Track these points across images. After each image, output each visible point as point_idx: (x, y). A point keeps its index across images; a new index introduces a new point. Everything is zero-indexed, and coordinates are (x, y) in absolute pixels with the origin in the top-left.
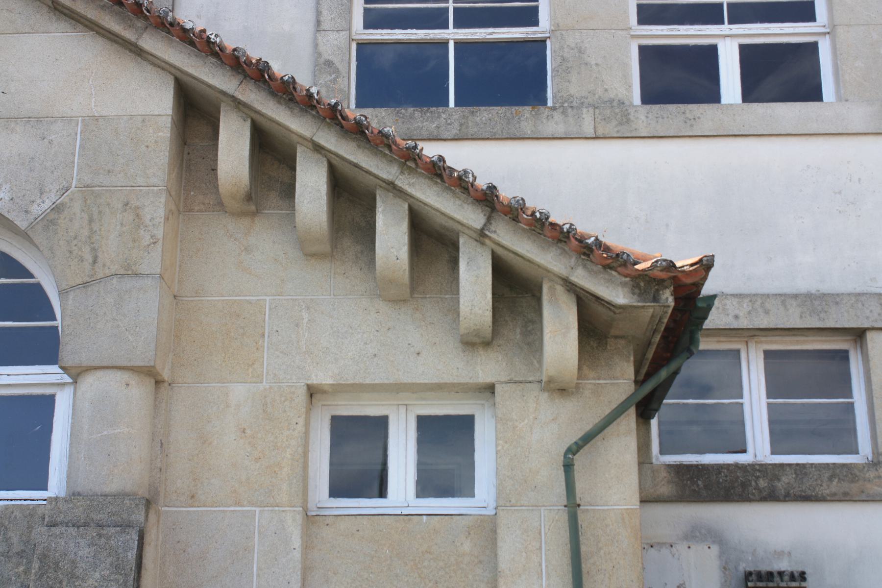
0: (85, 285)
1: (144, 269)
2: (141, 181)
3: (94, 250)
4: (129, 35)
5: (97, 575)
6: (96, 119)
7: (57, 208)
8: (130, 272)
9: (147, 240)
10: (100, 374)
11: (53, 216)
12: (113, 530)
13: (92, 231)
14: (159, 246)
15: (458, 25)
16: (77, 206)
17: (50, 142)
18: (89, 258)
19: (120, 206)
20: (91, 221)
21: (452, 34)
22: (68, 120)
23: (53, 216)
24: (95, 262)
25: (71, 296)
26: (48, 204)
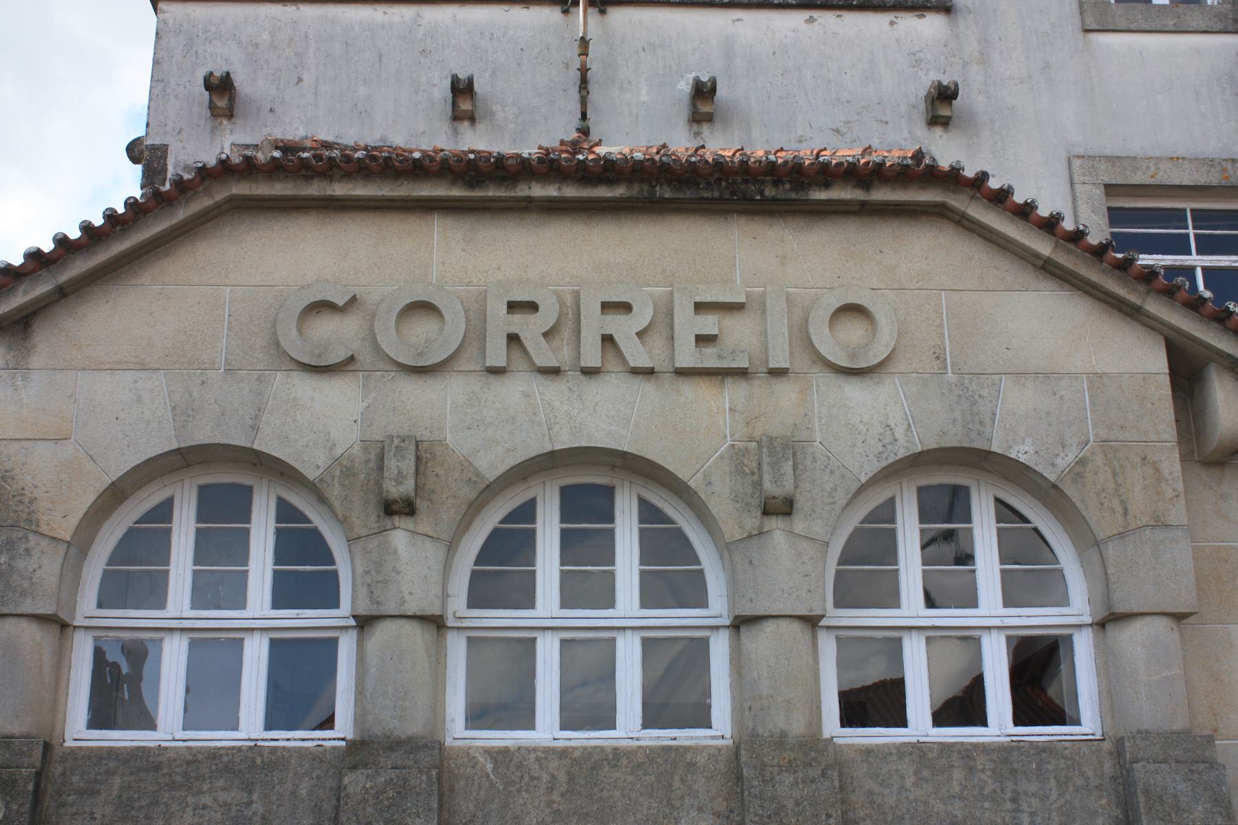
0: (1121, 535)
1: (1172, 520)
2: (1153, 437)
3: (1123, 502)
4: (1133, 298)
5: (1200, 808)
6: (1100, 376)
7: (1082, 462)
8: (1159, 524)
9: (1169, 494)
10: (1148, 619)
11: (1078, 469)
12: (1202, 766)
13: (1118, 485)
14: (1182, 500)
15: (1200, 252)
16: (1099, 460)
17: (1062, 397)
18: (1119, 509)
19: (1139, 460)
20: (1114, 474)
21: (1195, 259)
22: (1075, 376)
23: (1078, 469)
24: (1126, 513)
25: (1110, 545)
26: (1070, 458)
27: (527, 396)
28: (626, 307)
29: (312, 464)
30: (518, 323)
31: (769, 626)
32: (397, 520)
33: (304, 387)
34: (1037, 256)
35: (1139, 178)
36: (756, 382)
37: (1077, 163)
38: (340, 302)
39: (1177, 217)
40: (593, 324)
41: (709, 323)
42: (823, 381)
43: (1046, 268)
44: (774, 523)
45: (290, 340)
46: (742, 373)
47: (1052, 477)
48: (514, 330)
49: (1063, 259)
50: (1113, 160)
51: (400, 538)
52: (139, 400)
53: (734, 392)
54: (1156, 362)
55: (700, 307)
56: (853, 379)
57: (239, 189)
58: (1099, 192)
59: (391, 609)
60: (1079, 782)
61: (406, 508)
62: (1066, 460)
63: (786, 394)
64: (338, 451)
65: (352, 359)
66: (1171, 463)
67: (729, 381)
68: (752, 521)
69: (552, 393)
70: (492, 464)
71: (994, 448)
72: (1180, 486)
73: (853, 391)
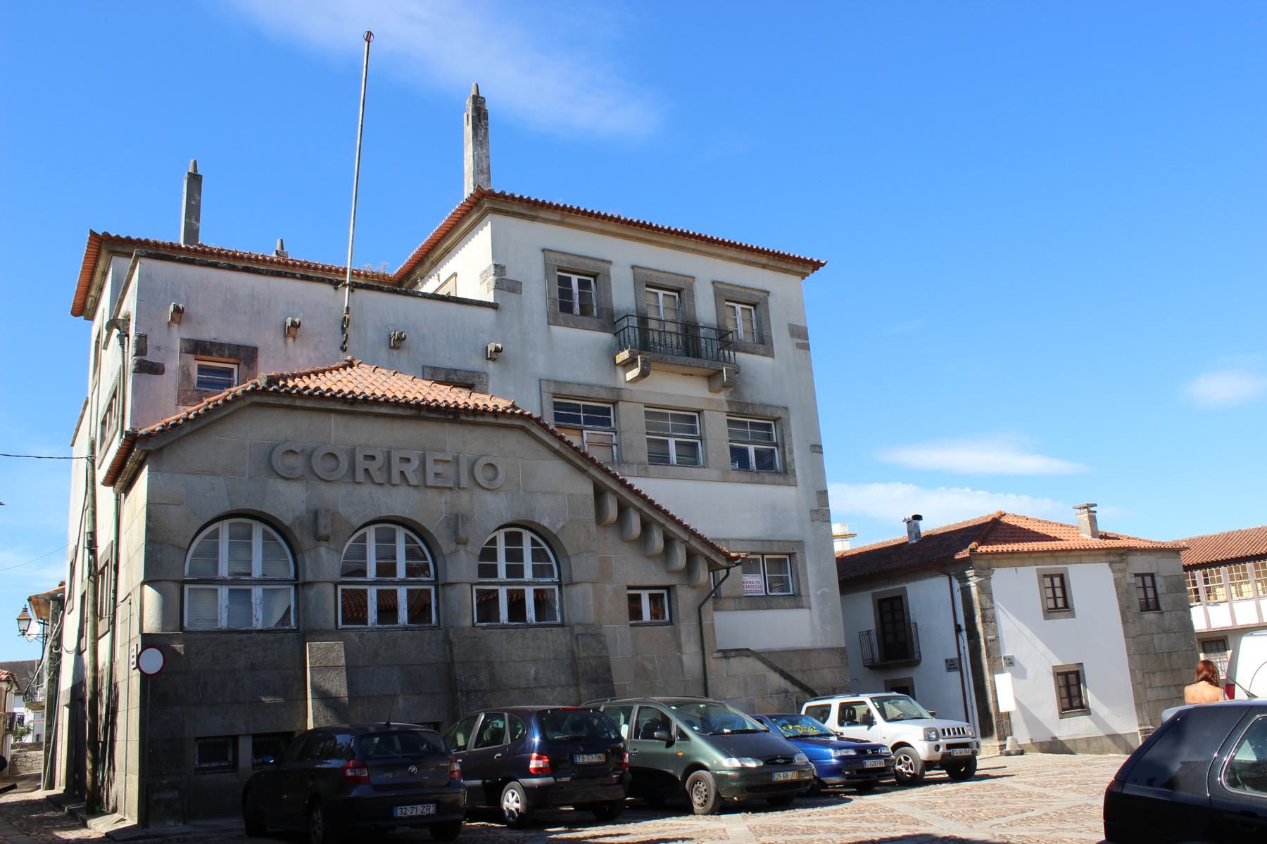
4: (585, 467)
6: (572, 494)
7: (563, 527)
27: (370, 493)
28: (408, 460)
29: (287, 519)
30: (368, 464)
31: (458, 586)
32: (322, 543)
33: (281, 486)
34: (554, 448)
35: (565, 392)
36: (454, 492)
37: (543, 382)
38: (297, 451)
39: (576, 408)
40: (396, 467)
41: (440, 468)
42: (477, 491)
43: (557, 453)
44: (461, 547)
45: (278, 463)
46: (450, 488)
47: (555, 532)
48: (366, 467)
49: (563, 451)
50: (557, 382)
51: (323, 550)
52: (213, 488)
53: (447, 496)
54: (590, 490)
55: (436, 461)
56: (489, 492)
57: (256, 399)
58: (550, 396)
59: (321, 579)
60: (560, 642)
61: (327, 539)
62: (559, 526)
63: (465, 497)
64: (297, 514)
65: (302, 476)
66: (593, 527)
67: (445, 491)
68: (453, 546)
69: (378, 493)
70: (357, 521)
71: (536, 520)
72: (596, 537)
73: (488, 497)
